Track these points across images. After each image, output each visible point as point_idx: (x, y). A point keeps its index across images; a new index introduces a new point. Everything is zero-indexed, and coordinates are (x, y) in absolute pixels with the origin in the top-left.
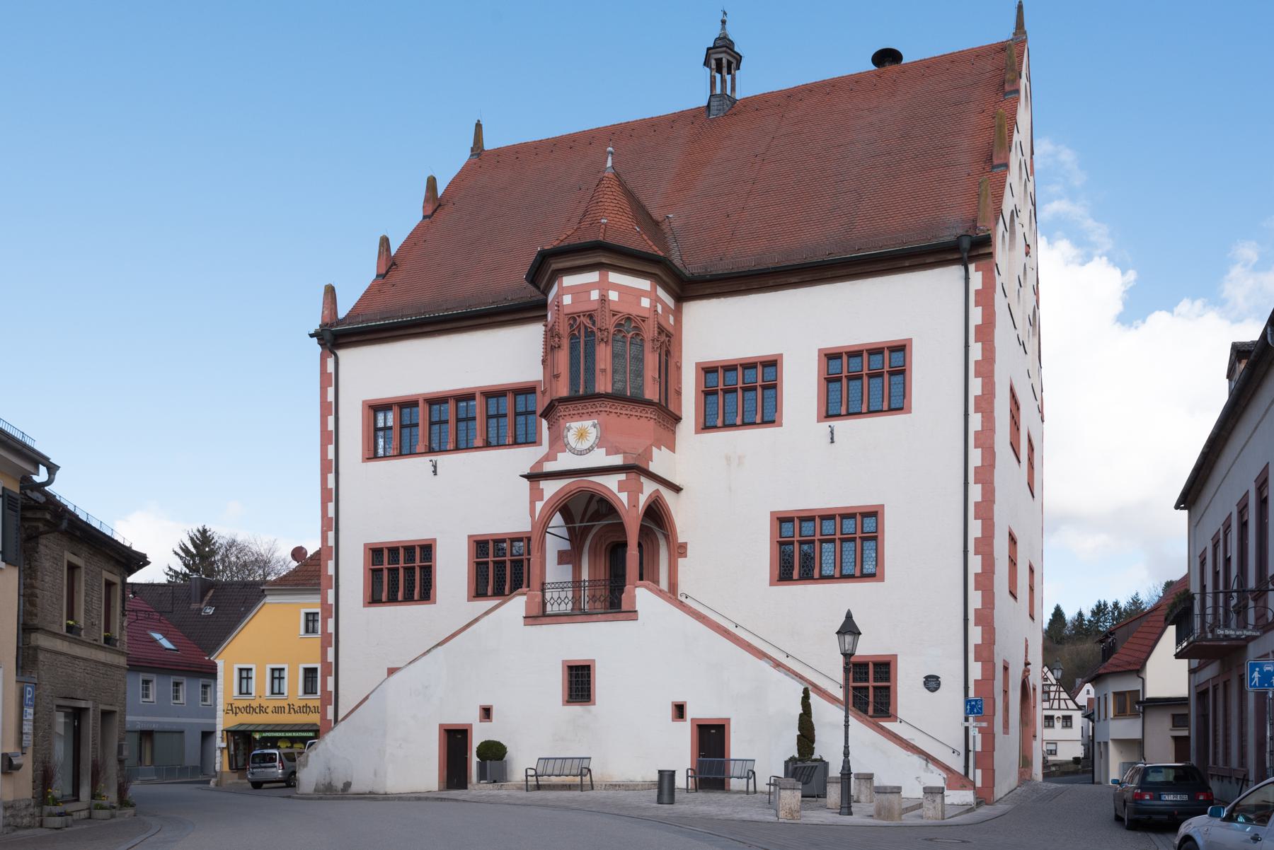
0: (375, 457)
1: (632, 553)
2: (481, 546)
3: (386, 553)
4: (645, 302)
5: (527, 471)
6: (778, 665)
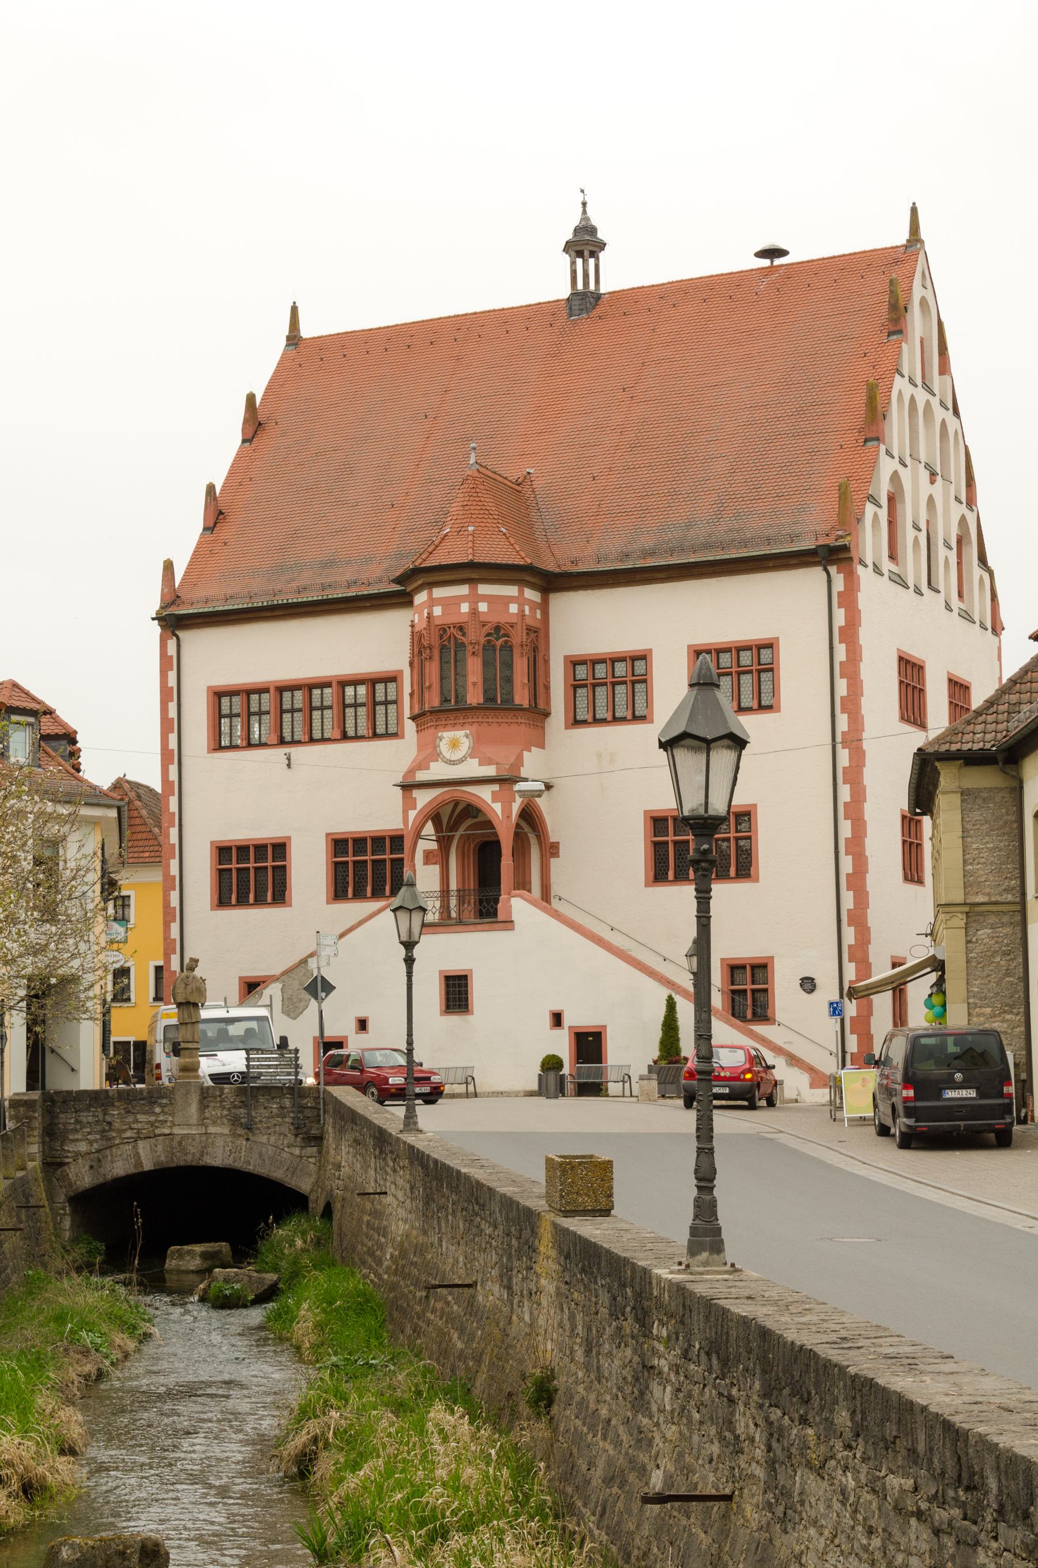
0: (219, 748)
1: (507, 863)
3: (234, 851)
4: (513, 608)
5: (399, 780)
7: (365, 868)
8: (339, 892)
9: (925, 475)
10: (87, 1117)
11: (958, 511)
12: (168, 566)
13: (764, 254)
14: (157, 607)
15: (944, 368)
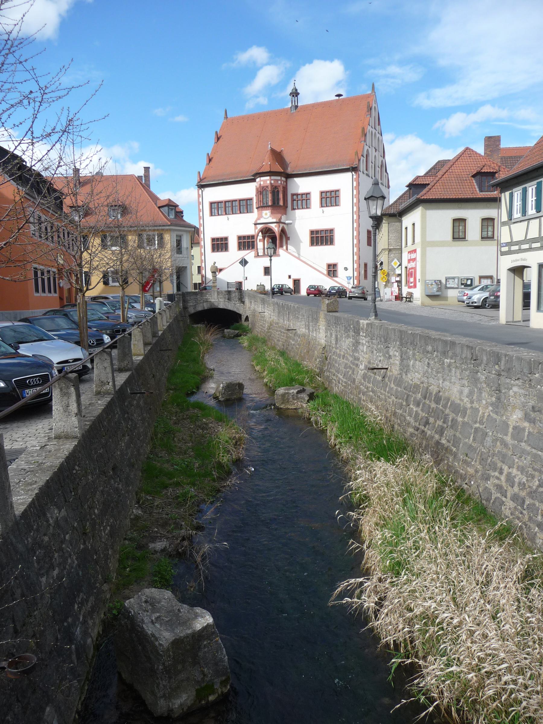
2: (239, 238)
4: (279, 182)
6: (311, 266)
7: (246, 243)
8: (240, 249)
9: (374, 150)
10: (192, 297)
11: (381, 159)
12: (199, 173)
13: (337, 96)
14: (196, 182)
15: (379, 124)
